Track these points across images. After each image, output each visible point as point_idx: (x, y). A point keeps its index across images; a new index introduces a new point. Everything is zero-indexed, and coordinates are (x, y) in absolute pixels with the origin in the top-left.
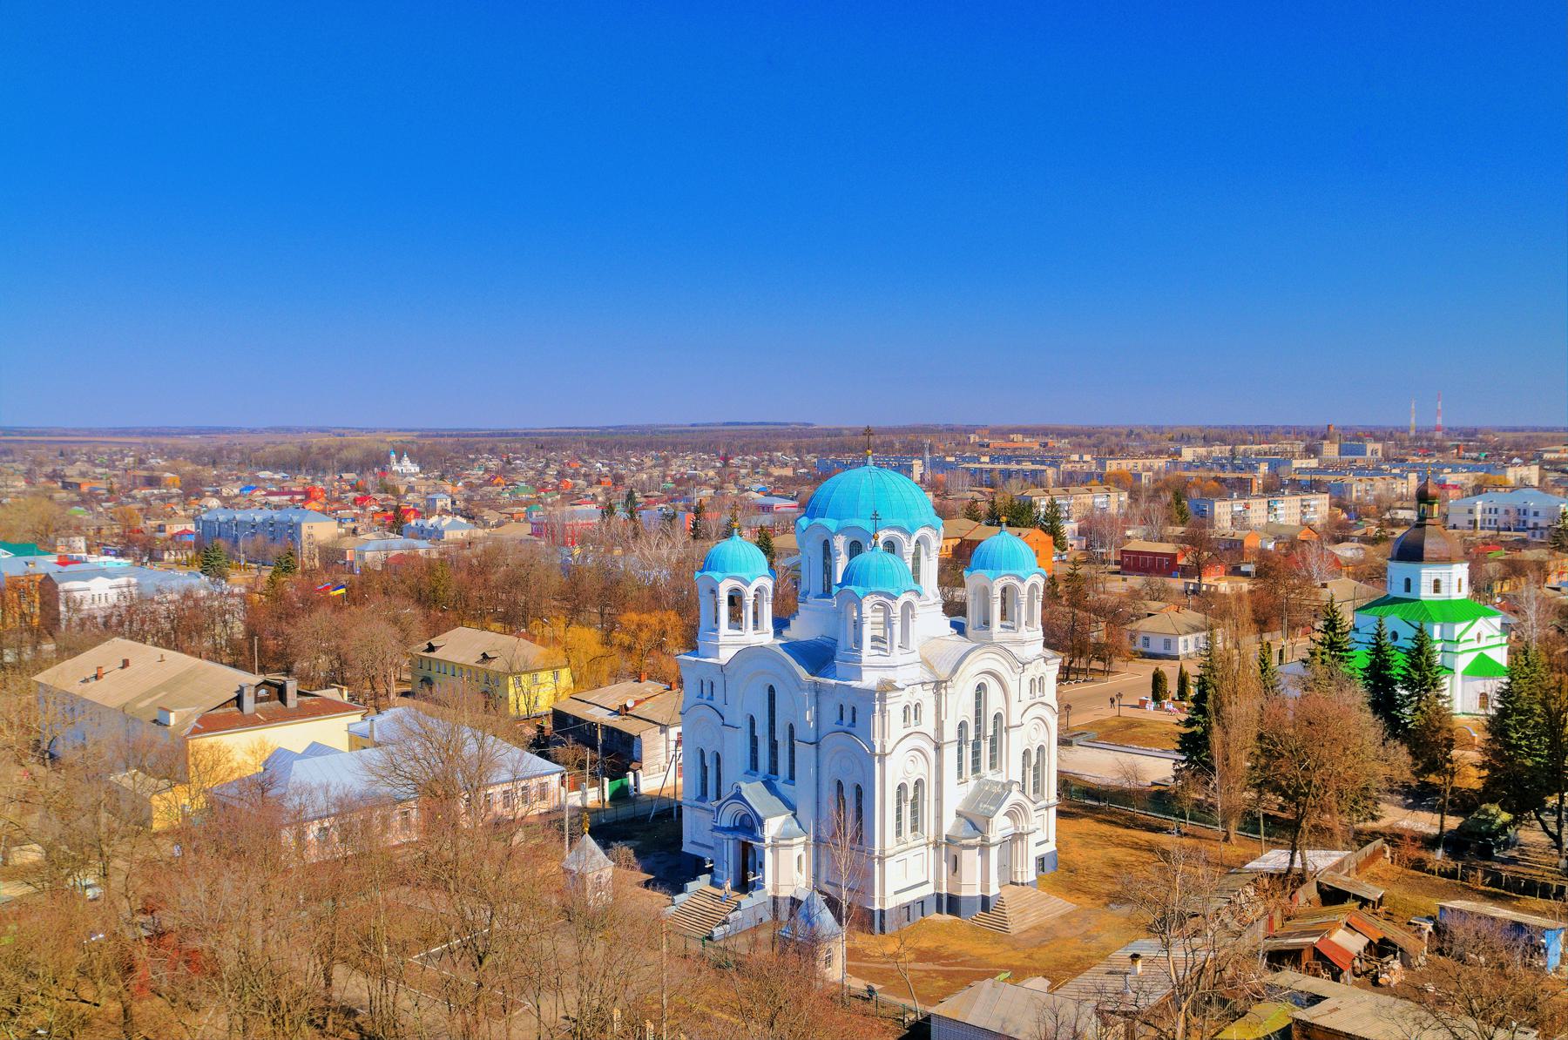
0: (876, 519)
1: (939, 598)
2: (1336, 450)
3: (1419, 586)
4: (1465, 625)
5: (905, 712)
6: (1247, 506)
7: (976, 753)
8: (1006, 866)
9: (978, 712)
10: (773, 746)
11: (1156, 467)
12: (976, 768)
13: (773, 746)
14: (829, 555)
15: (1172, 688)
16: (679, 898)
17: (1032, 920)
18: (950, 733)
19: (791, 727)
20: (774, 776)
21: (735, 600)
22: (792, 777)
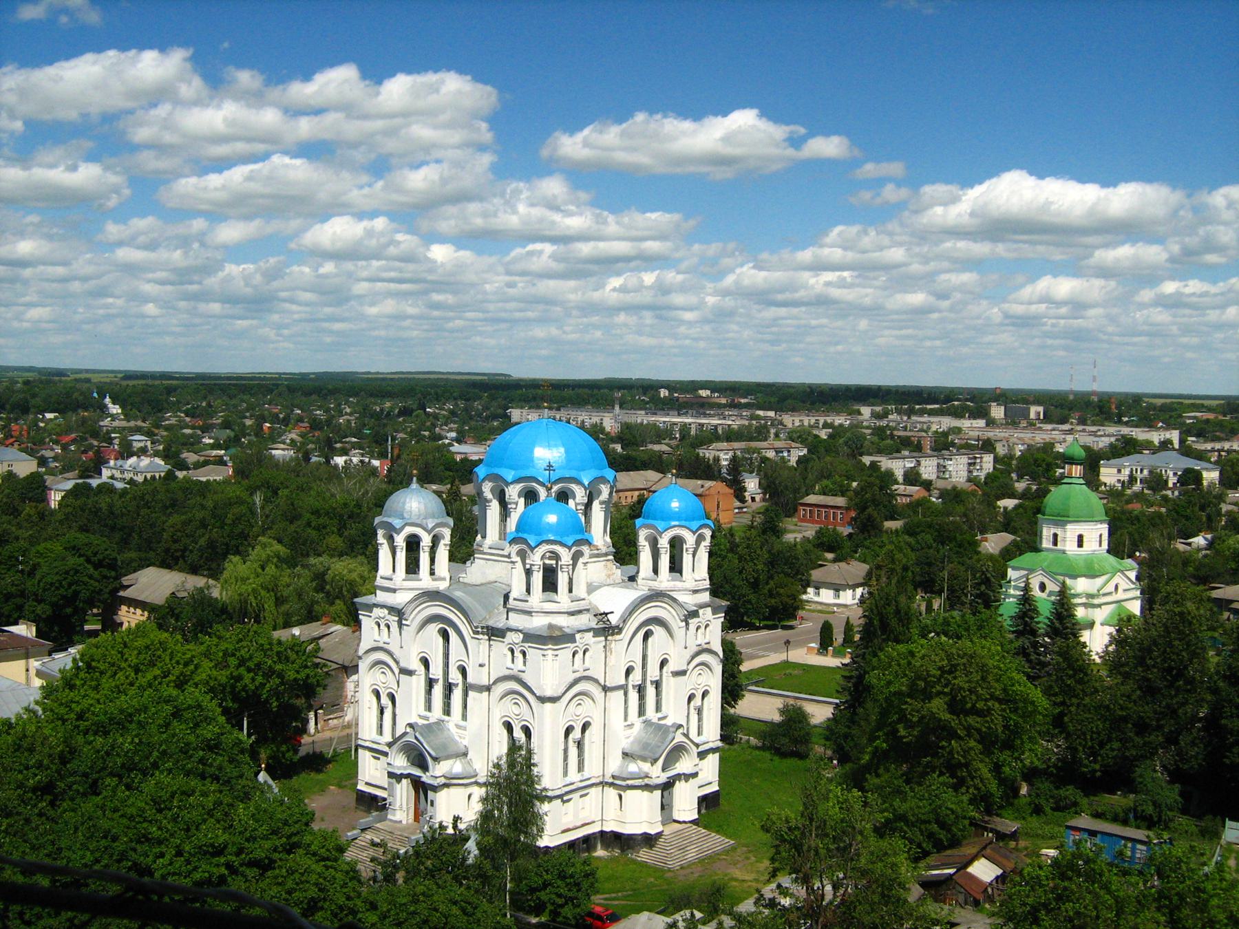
2: (1003, 412)
3: (1064, 540)
4: (1104, 578)
6: (919, 463)
8: (665, 807)
9: (644, 657)
11: (836, 424)
12: (642, 711)
13: (449, 688)
15: (839, 638)
16: (881, 843)
17: (692, 854)
20: (446, 718)
21: (413, 544)
22: (464, 717)
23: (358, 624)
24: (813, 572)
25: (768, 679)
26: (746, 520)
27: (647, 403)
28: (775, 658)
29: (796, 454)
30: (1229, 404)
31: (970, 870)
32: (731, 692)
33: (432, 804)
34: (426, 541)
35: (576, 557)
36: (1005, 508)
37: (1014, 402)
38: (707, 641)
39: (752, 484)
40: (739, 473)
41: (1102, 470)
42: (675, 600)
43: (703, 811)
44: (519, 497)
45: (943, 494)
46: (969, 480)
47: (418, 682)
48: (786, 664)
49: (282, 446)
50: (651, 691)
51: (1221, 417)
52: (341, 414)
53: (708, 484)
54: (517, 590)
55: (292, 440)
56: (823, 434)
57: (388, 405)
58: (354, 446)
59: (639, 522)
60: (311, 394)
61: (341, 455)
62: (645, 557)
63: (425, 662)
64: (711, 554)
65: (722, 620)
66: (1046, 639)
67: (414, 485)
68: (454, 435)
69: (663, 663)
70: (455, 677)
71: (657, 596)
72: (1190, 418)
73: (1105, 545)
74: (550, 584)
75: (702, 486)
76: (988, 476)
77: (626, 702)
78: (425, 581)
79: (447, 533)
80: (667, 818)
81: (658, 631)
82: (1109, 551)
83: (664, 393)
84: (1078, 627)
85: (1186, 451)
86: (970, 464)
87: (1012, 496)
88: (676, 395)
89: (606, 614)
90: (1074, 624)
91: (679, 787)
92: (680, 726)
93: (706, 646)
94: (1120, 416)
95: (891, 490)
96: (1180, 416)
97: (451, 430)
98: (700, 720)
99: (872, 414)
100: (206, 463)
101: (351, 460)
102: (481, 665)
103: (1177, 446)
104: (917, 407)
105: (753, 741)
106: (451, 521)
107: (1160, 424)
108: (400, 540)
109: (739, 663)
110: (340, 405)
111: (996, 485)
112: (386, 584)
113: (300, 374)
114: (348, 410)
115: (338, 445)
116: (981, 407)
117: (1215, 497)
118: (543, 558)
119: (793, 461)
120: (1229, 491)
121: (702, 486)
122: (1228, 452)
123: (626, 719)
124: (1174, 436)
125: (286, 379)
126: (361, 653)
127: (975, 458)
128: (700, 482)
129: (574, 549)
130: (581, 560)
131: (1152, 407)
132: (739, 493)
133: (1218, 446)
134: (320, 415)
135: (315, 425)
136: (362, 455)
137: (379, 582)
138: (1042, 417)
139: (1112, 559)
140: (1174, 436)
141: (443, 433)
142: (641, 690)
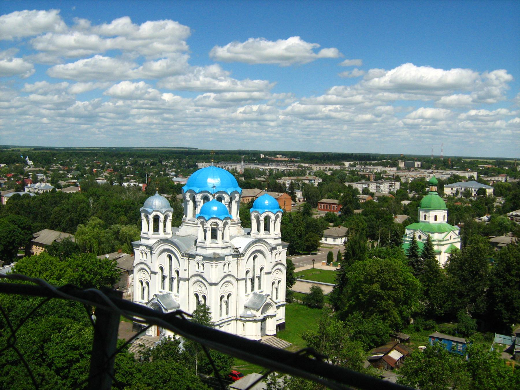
3: (429, 217)
6: (369, 186)
7: (253, 283)
8: (263, 329)
9: (254, 267)
11: (334, 169)
12: (253, 289)
13: (172, 280)
15: (335, 258)
16: (352, 343)
20: (170, 292)
21: (156, 219)
22: (178, 292)
24: (324, 231)
25: (305, 275)
26: (296, 209)
27: (255, 160)
28: (308, 267)
29: (317, 182)
30: (497, 161)
31: (390, 355)
32: (290, 281)
34: (162, 218)
35: (225, 225)
36: (405, 204)
37: (408, 160)
38: (280, 260)
39: (299, 194)
40: (294, 190)
41: (445, 189)
42: (266, 242)
43: (278, 331)
44: (201, 199)
45: (379, 198)
46: (390, 193)
47: (159, 277)
48: (313, 269)
49: (101, 178)
50: (256, 281)
51: (494, 167)
52: (126, 165)
53: (281, 194)
54: (200, 238)
55: (105, 176)
56: (329, 173)
57: (146, 161)
58: (132, 178)
59: (251, 210)
60: (113, 157)
61: (126, 182)
62: (254, 224)
63: (162, 269)
64: (282, 223)
65: (286, 251)
66: (421, 259)
67: (157, 194)
68: (174, 173)
69: (262, 269)
70: (174, 275)
71: (259, 241)
72: (481, 167)
73: (446, 220)
74: (214, 236)
75: (278, 195)
76: (397, 191)
77: (246, 285)
78: (161, 234)
79: (171, 214)
80: (263, 334)
81: (259, 255)
82: (447, 222)
83: (262, 156)
84: (434, 254)
85: (479, 181)
86: (390, 186)
87: (407, 199)
88: (267, 157)
89: (238, 248)
90: (433, 253)
91: (268, 321)
92: (269, 295)
94: (452, 166)
95: (357, 196)
96: (477, 166)
97: (173, 172)
98: (277, 293)
99: (349, 165)
100: (69, 185)
101: (130, 184)
102: (185, 270)
103: (476, 179)
104: (368, 162)
105: (299, 301)
106: (172, 210)
107: (469, 170)
108: (151, 217)
109: (293, 269)
110: (126, 161)
111: (401, 195)
112: (145, 236)
113: (109, 148)
114: (129, 163)
115: (125, 178)
116: (395, 162)
117: (491, 200)
118: (211, 225)
119: (316, 185)
120: (497, 198)
121: (278, 195)
122: (497, 181)
123: (246, 292)
124: (475, 174)
125: (103, 150)
126: (134, 265)
127: (392, 183)
128: (277, 193)
130: (227, 226)
131: (465, 162)
132: (294, 198)
133: (493, 179)
134: (118, 165)
135: (115, 169)
136: (135, 182)
137: (142, 235)
138: (420, 166)
139: (449, 226)
140: (475, 174)
141: (169, 173)
142: (252, 280)
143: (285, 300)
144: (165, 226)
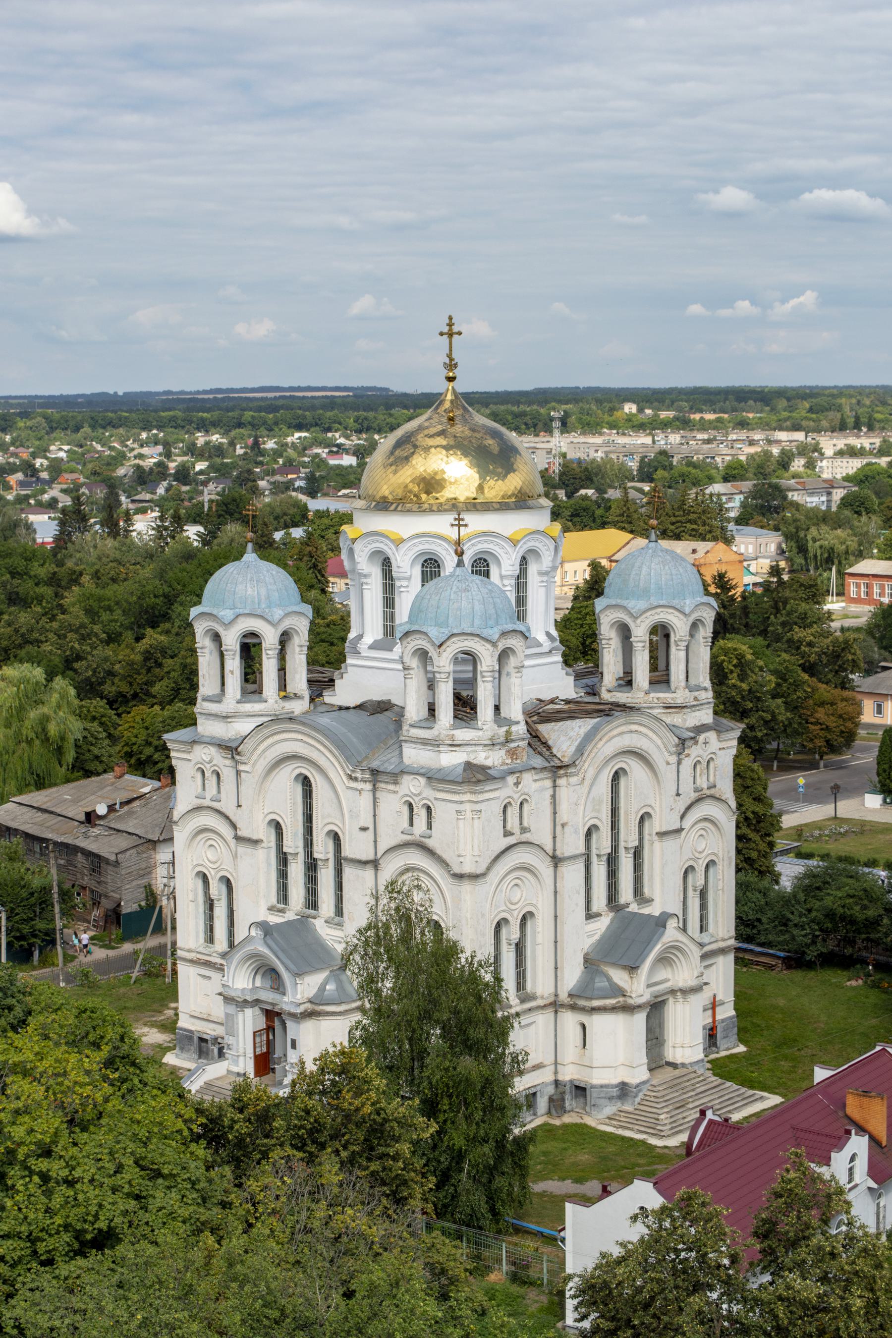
0: (459, 526)
1: (557, 643)
5: (504, 811)
9: (614, 812)
10: (312, 866)
13: (312, 866)
14: (392, 578)
18: (573, 844)
19: (336, 838)
20: (311, 912)
22: (339, 912)
23: (172, 771)
33: (294, 1045)
35: (504, 656)
54: (414, 710)
59: (599, 604)
63: (278, 827)
65: (734, 751)
81: (635, 768)
93: (708, 792)
98: (703, 907)
106: (308, 610)
126: (176, 816)
129: (501, 646)
130: (513, 661)
137: (201, 706)
142: (612, 861)
143: (733, 933)
144: (282, 669)
